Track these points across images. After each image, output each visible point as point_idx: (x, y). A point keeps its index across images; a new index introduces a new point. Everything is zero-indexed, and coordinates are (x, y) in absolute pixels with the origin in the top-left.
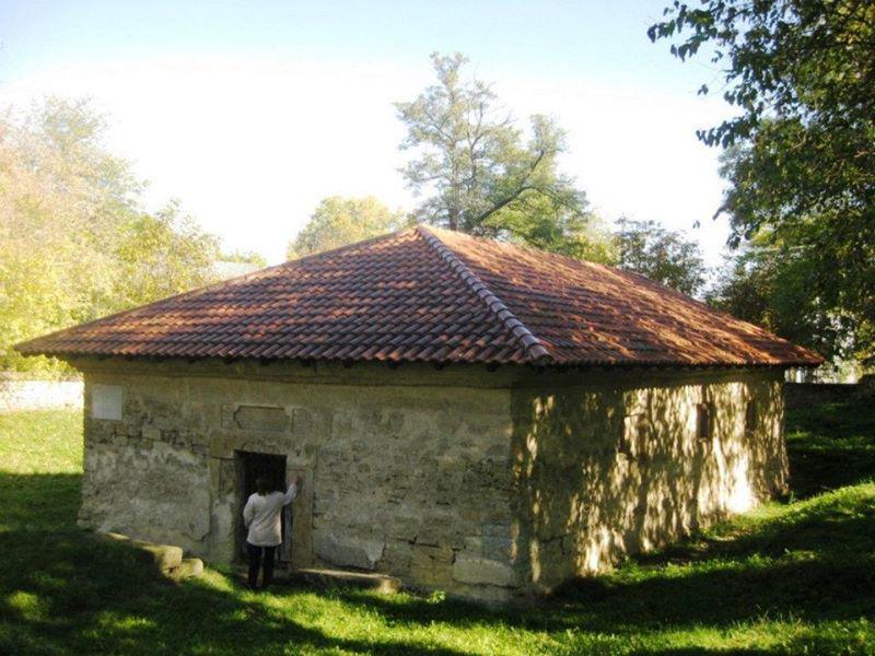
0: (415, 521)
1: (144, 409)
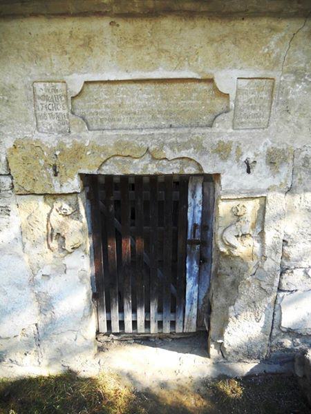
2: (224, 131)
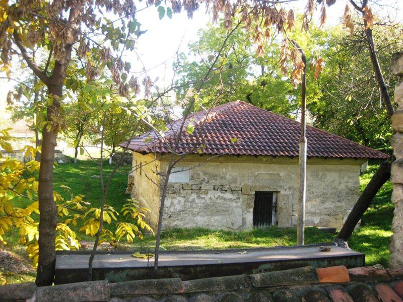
0: (331, 208)
1: (202, 176)
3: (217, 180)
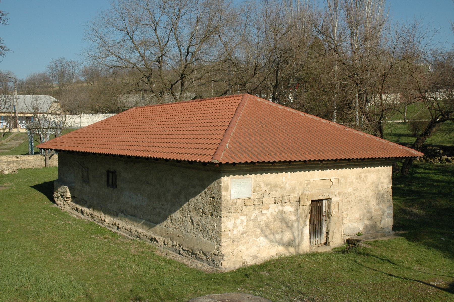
2: (332, 189)
3: (278, 190)
